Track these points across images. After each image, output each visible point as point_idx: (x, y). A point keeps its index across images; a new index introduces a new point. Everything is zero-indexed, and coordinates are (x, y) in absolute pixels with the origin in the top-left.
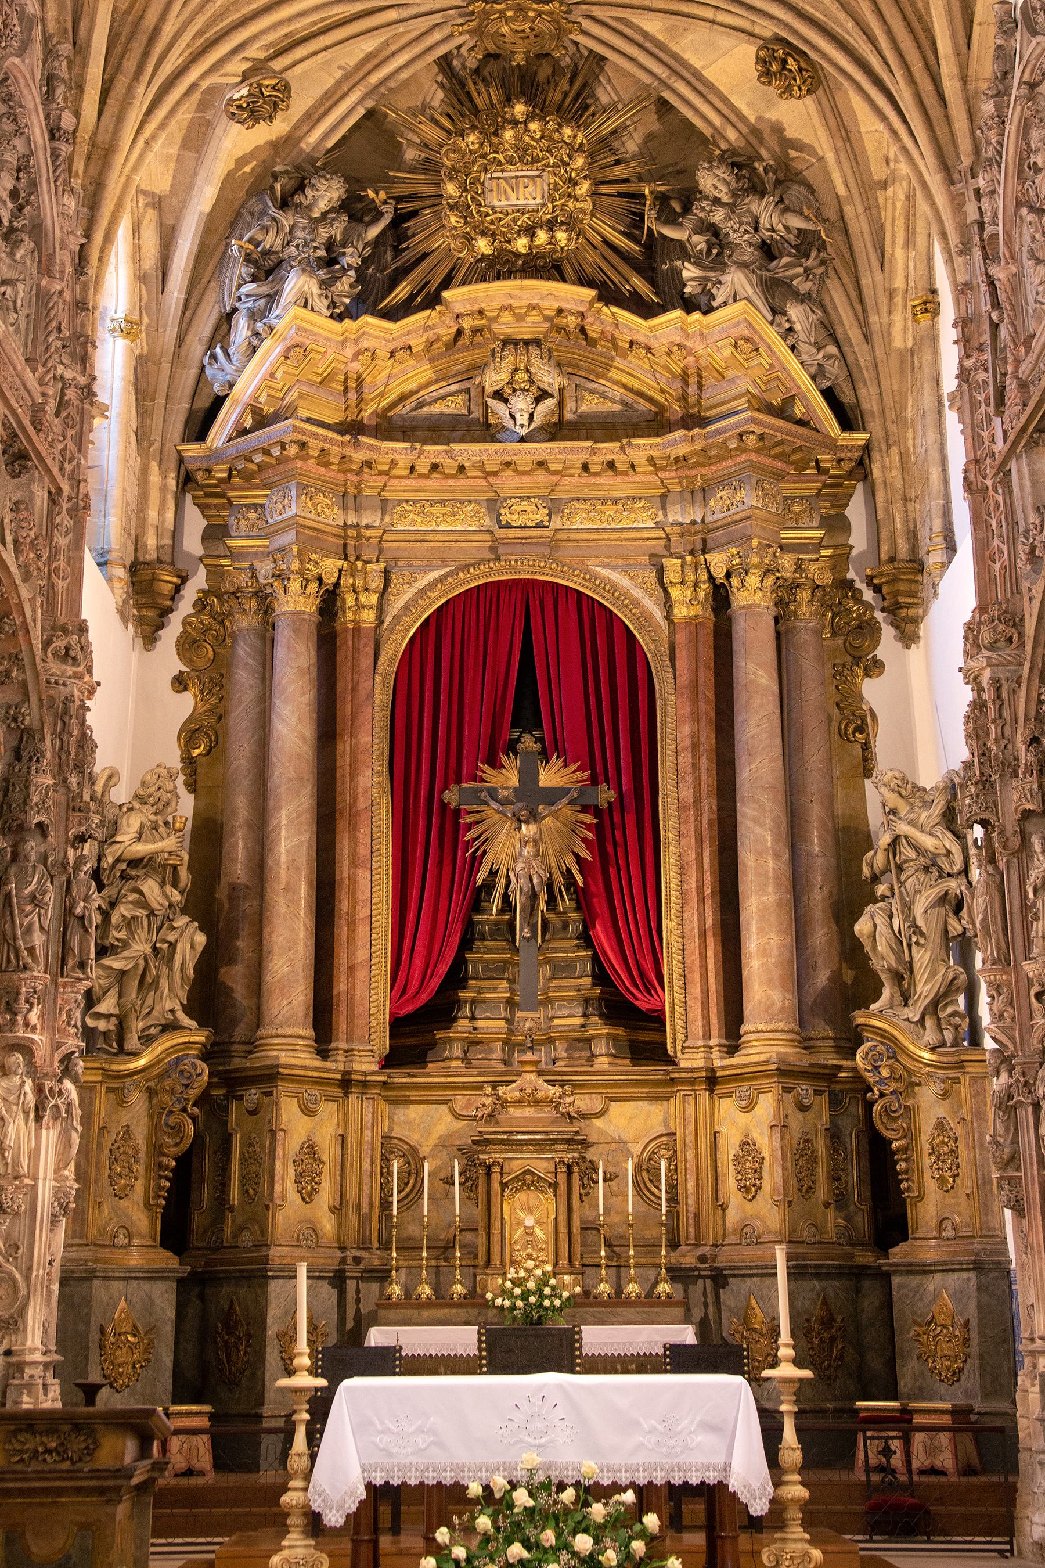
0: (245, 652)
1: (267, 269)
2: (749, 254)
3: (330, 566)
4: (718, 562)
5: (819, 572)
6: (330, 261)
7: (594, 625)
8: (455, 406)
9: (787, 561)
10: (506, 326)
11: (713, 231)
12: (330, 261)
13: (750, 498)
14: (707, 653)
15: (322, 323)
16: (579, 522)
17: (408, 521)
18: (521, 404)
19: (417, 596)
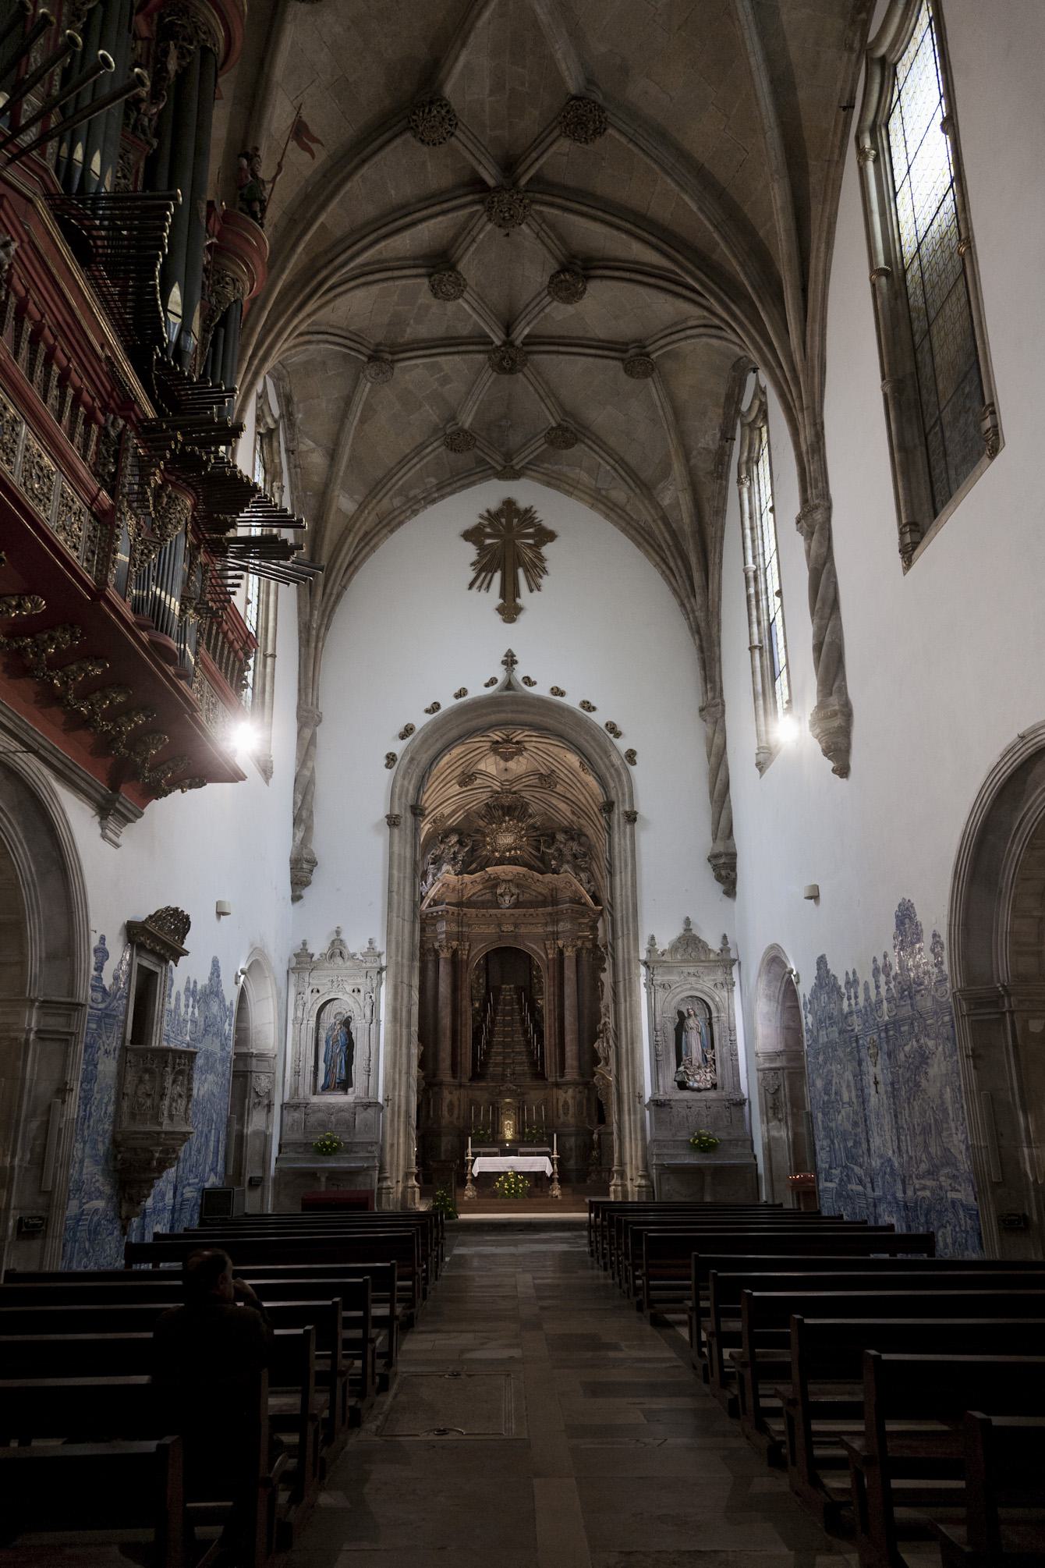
0: (430, 966)
1: (437, 861)
2: (569, 858)
3: (455, 944)
4: (560, 943)
5: (589, 945)
6: (454, 858)
8: (488, 897)
9: (579, 943)
10: (503, 876)
11: (559, 850)
12: (454, 858)
13: (569, 926)
15: (452, 878)
16: (523, 930)
17: (476, 930)
18: (507, 898)
19: (476, 953)
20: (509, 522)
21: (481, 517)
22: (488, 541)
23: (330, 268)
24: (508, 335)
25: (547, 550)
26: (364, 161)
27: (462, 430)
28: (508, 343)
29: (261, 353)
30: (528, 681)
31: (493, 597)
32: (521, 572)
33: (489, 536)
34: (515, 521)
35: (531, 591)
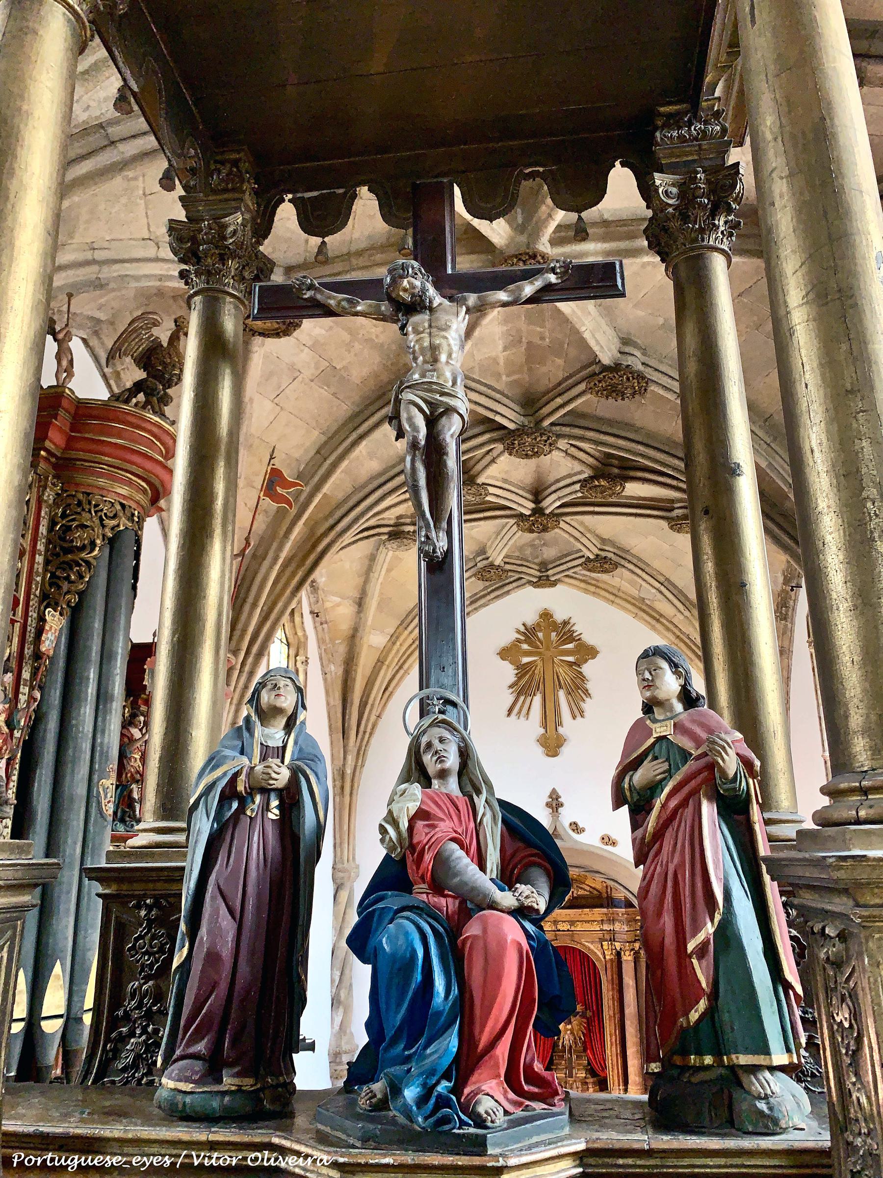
7: (584, 959)
14: (615, 969)
20: (547, 636)
21: (518, 632)
22: (526, 660)
23: (333, 534)
24: (537, 500)
25: (587, 669)
26: (361, 437)
27: (492, 565)
28: (538, 511)
29: (255, 649)
30: (575, 827)
31: (533, 726)
32: (562, 694)
33: (527, 654)
34: (554, 634)
35: (574, 717)
